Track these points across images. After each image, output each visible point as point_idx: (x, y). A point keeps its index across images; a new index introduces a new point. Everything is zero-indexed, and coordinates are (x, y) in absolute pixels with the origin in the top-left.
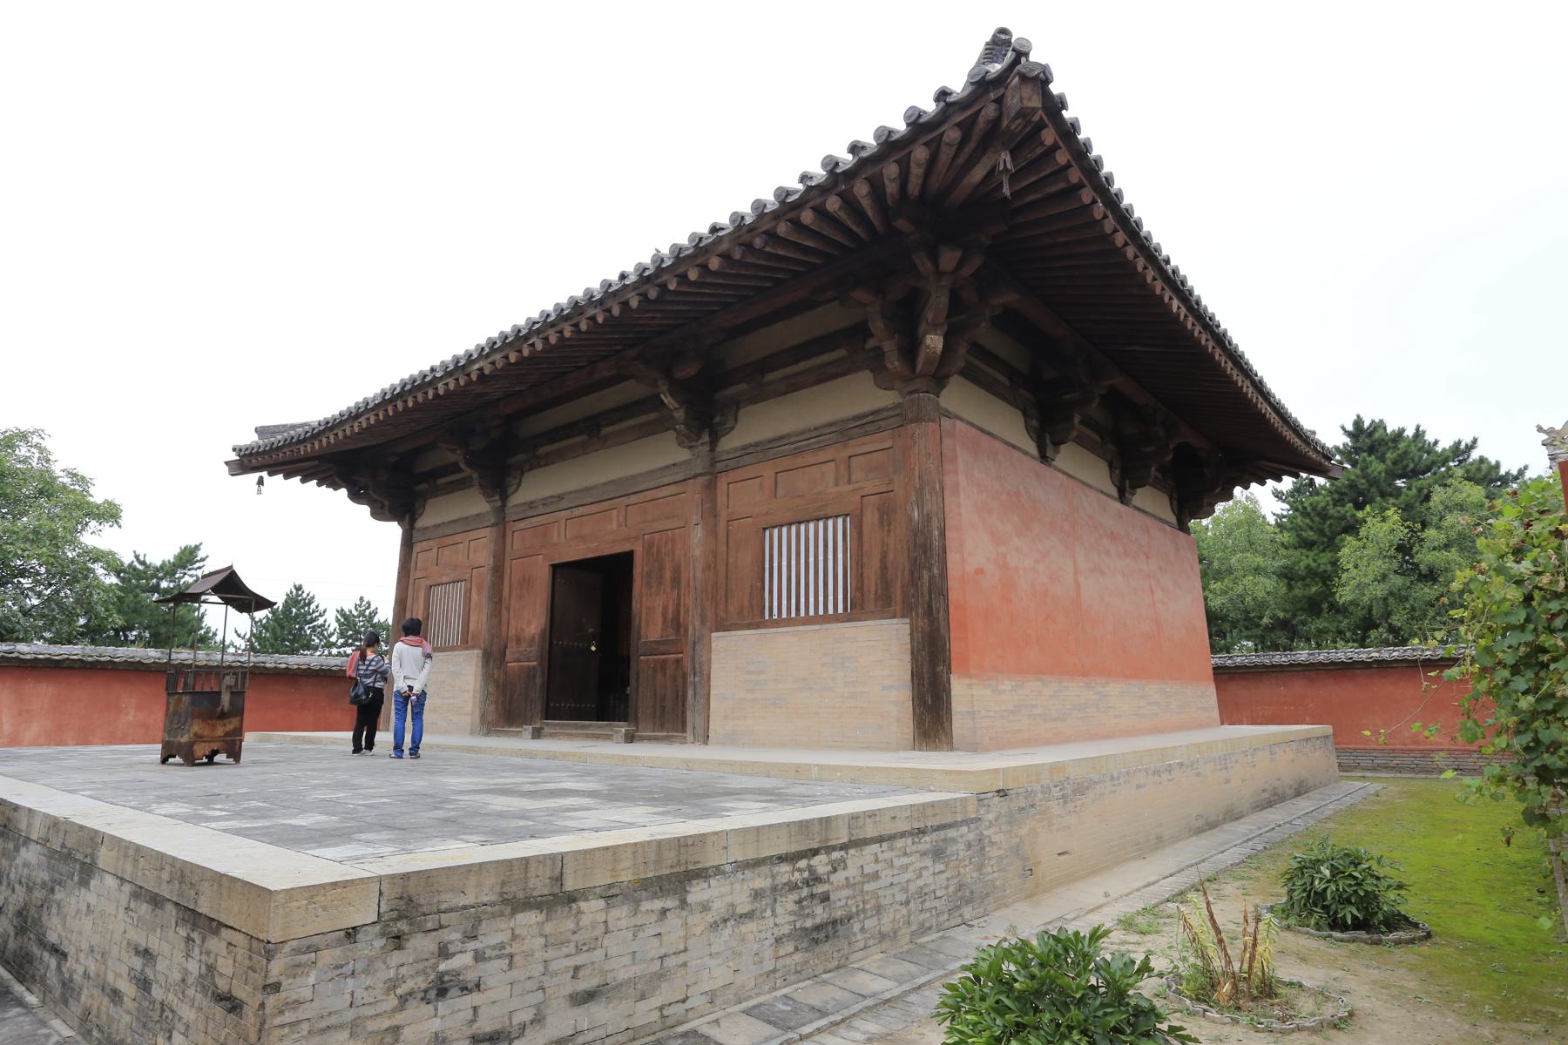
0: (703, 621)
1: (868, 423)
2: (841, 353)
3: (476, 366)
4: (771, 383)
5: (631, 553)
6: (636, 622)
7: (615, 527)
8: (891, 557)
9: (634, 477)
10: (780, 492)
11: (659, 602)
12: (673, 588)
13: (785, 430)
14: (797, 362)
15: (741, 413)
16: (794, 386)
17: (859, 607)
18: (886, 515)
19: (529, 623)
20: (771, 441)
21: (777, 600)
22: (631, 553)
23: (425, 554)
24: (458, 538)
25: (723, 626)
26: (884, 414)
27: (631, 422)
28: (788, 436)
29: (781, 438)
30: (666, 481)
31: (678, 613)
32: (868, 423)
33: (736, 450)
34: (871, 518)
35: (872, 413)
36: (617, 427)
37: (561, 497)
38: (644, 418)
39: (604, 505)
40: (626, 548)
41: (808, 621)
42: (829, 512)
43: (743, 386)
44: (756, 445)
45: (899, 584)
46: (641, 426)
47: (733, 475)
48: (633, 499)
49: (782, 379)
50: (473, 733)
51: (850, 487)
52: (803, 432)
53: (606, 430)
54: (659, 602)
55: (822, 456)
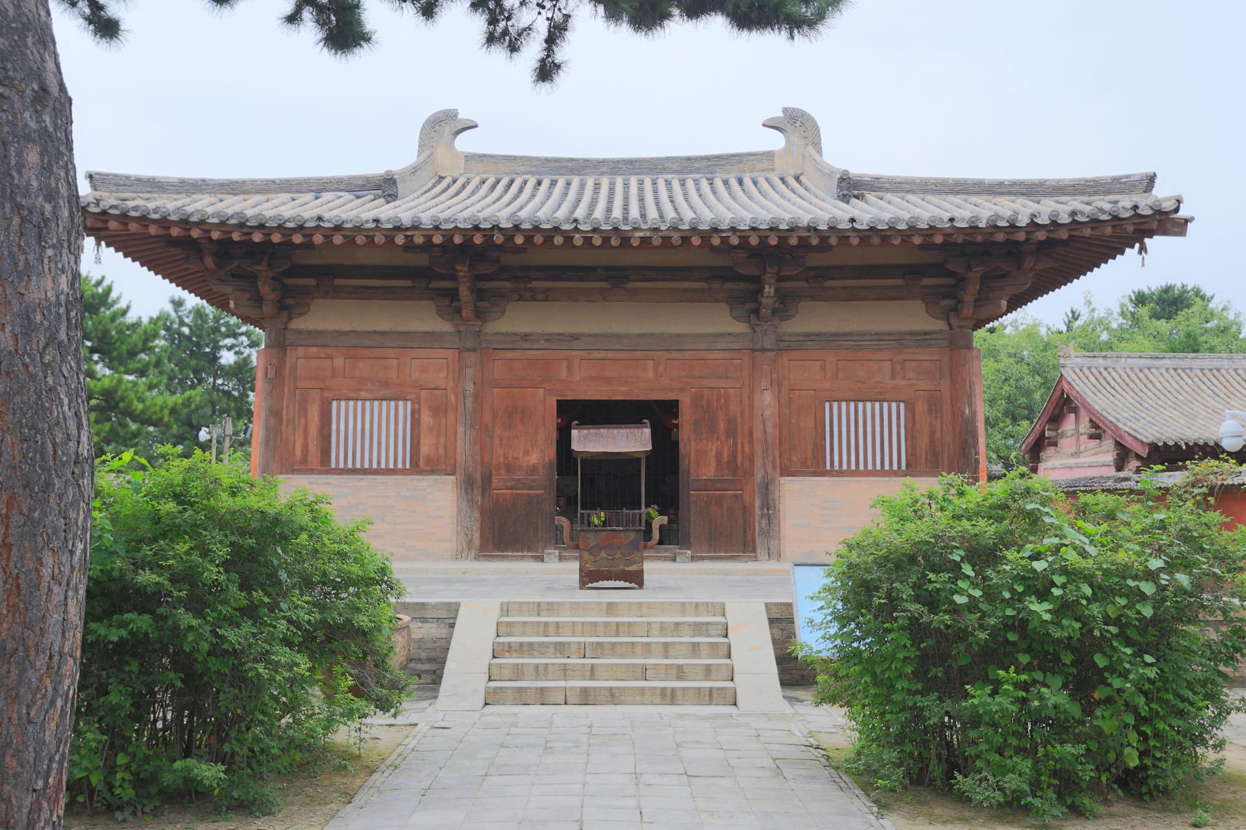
0: (774, 468)
1: (922, 339)
2: (900, 282)
3: (641, 234)
4: (833, 288)
5: (675, 403)
6: (683, 464)
7: (651, 375)
8: (938, 435)
9: (679, 336)
10: (841, 375)
11: (712, 448)
12: (727, 437)
13: (847, 329)
14: (860, 278)
15: (801, 305)
16: (854, 296)
17: (912, 468)
18: (934, 405)
19: (526, 453)
20: (833, 335)
21: (837, 455)
22: (675, 403)
23: (298, 358)
24: (391, 353)
25: (786, 472)
26: (934, 336)
27: (669, 285)
28: (849, 334)
29: (844, 334)
30: (720, 346)
31: (735, 458)
32: (922, 339)
33: (798, 335)
34: (921, 407)
35: (926, 334)
36: (649, 285)
37: (575, 337)
38: (686, 285)
39: (638, 354)
40: (670, 396)
41: (874, 473)
42: (887, 396)
43: (804, 284)
44: (819, 335)
45: (945, 455)
46: (685, 290)
47: (794, 355)
48: (675, 355)
49: (844, 288)
50: (458, 556)
51: (905, 382)
52: (864, 335)
53: (630, 285)
54: (712, 448)
55: (880, 356)
